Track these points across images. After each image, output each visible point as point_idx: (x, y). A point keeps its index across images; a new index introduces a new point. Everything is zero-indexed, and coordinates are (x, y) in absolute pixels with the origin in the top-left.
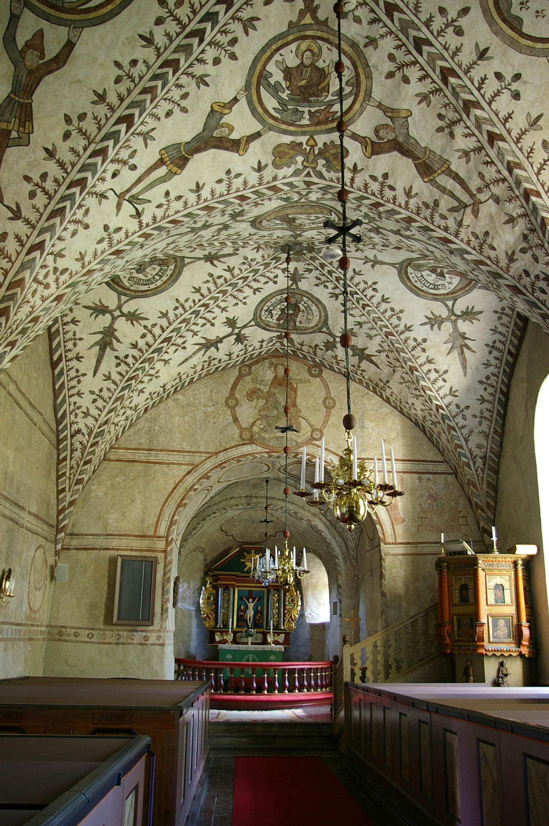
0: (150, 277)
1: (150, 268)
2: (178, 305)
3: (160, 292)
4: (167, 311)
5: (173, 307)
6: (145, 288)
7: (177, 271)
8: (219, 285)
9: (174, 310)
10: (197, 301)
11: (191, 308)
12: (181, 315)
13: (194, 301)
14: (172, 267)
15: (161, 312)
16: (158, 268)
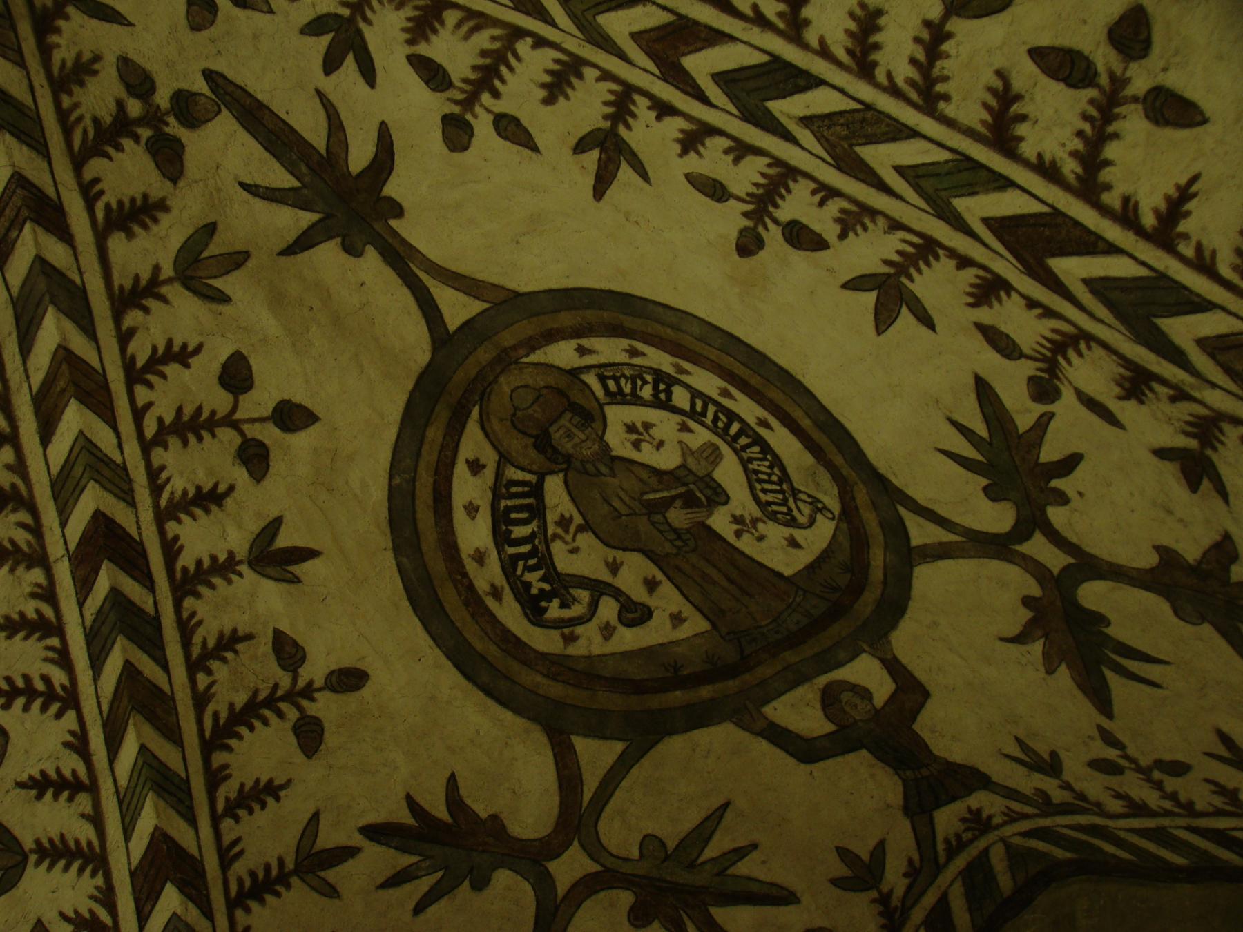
0: (701, 436)
1: (647, 455)
2: (773, 236)
3: (757, 358)
4: (856, 284)
5: (798, 258)
6: (782, 440)
7: (566, 319)
8: (483, 39)
9: (819, 244)
10: (674, 126)
11: (741, 150)
12: (827, 193)
13: (691, 142)
14: (563, 354)
15: (883, 320)
16: (617, 415)
